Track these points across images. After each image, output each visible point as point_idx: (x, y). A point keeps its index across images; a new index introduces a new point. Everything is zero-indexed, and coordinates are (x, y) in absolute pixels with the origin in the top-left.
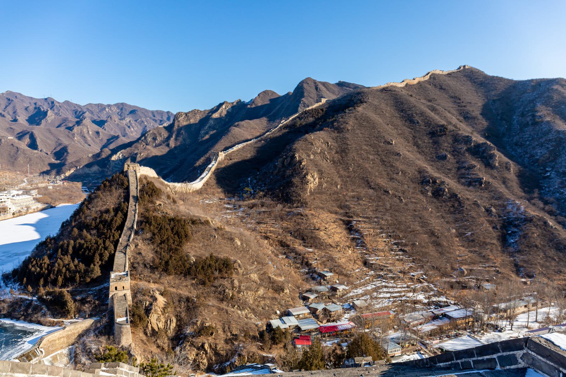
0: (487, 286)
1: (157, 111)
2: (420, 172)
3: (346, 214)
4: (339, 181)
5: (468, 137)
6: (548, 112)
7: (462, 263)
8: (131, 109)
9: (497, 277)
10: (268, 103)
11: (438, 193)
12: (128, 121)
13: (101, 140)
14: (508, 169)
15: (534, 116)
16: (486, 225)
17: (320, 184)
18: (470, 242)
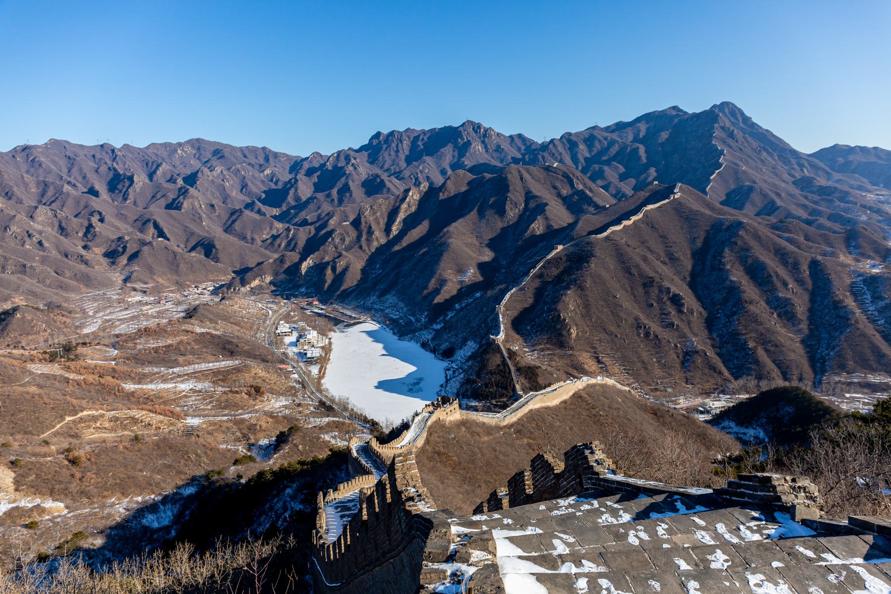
0: (669, 390)
1: (247, 147)
2: (636, 320)
3: (595, 353)
4: (587, 329)
5: (669, 288)
6: (732, 258)
7: (658, 378)
8: (213, 149)
9: (674, 386)
10: (464, 188)
11: (647, 334)
12: (219, 171)
13: (219, 216)
14: (693, 313)
15: (720, 261)
16: (674, 356)
17: (578, 334)
18: (664, 366)
